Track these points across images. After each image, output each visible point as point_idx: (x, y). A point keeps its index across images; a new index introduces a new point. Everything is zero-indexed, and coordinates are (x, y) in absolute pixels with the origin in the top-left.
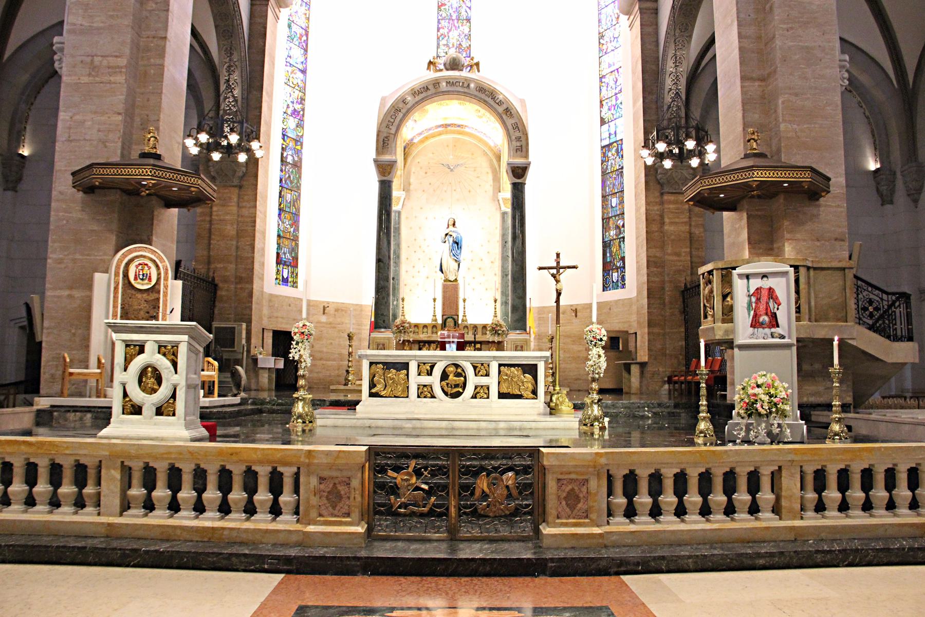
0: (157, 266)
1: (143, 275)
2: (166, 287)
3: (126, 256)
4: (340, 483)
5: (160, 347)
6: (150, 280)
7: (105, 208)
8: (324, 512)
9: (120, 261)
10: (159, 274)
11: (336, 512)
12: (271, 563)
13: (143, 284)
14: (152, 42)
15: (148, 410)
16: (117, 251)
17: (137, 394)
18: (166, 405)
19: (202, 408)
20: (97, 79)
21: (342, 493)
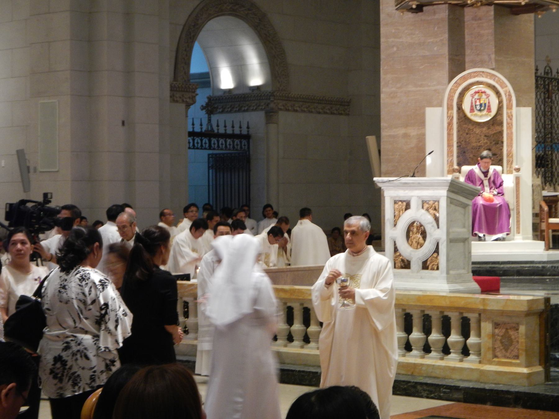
0: (498, 93)
1: (481, 105)
2: (510, 117)
3: (460, 85)
4: (510, 329)
5: (423, 202)
6: (489, 110)
7: (436, 29)
8: (498, 354)
9: (453, 91)
10: (500, 102)
11: (508, 354)
12: (444, 393)
13: (481, 116)
15: (416, 265)
16: (451, 79)
17: (406, 250)
18: (430, 259)
19: (474, 263)
21: (513, 337)
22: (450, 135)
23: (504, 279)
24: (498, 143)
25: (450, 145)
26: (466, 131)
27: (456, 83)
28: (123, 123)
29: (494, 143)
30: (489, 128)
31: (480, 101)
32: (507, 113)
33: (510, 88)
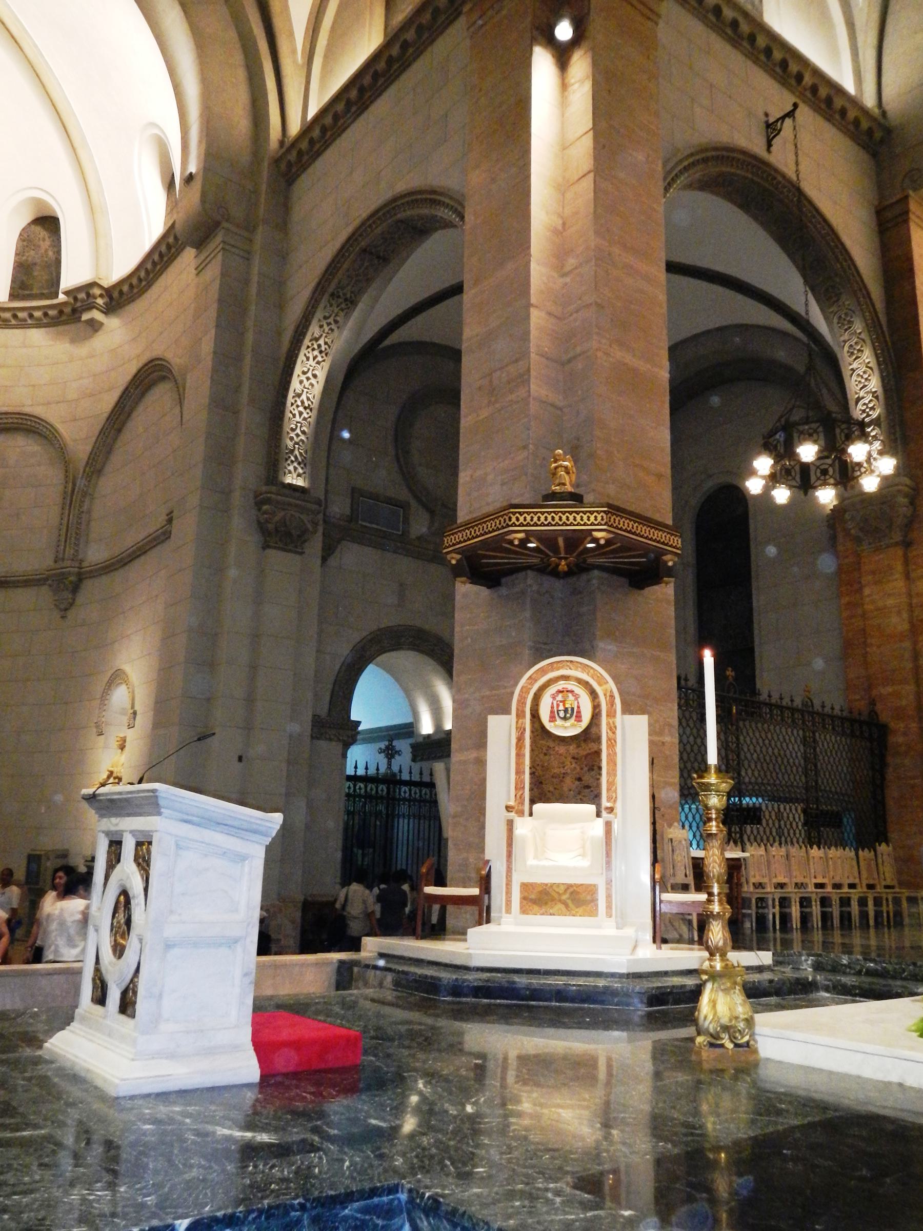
0: (593, 694)
1: (566, 710)
2: (612, 729)
6: (579, 718)
9: (524, 691)
10: (596, 708)
14: (575, 320)
20: (497, 405)
22: (520, 755)
23: (533, 1006)
24: (593, 770)
25: (519, 772)
26: (544, 751)
27: (530, 677)
28: (240, 759)
29: (586, 769)
30: (578, 746)
31: (564, 705)
32: (608, 724)
33: (612, 685)
